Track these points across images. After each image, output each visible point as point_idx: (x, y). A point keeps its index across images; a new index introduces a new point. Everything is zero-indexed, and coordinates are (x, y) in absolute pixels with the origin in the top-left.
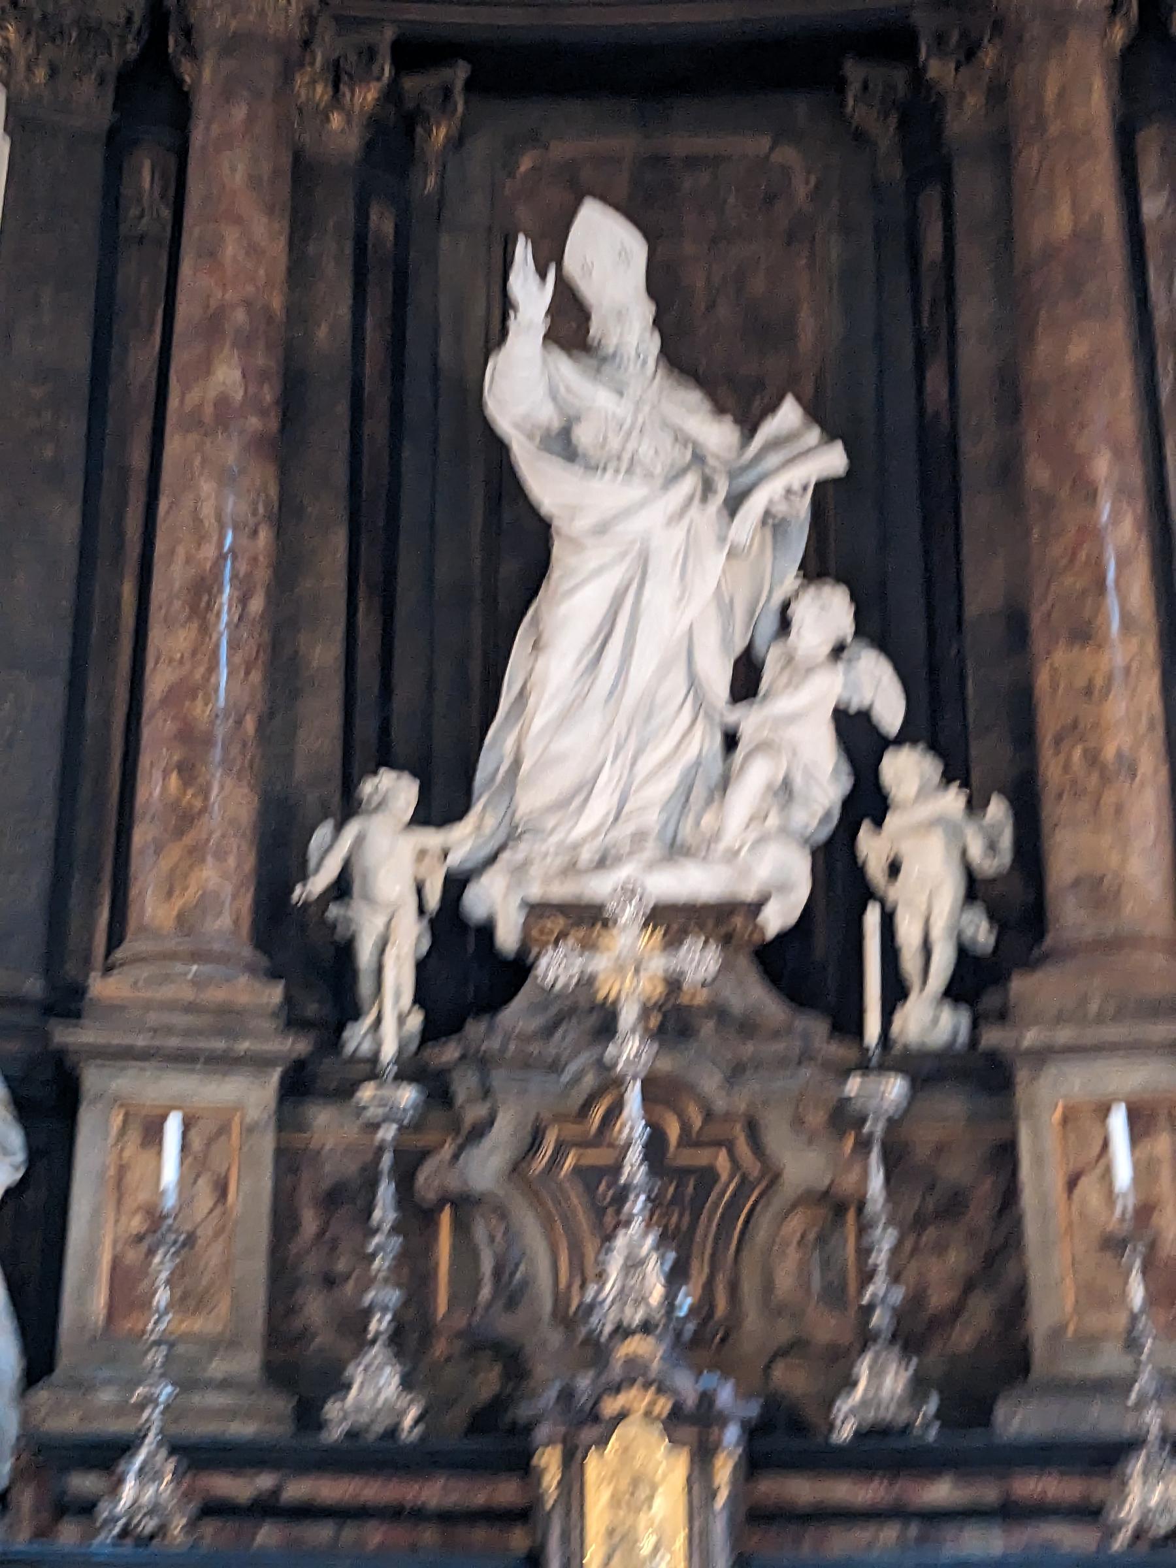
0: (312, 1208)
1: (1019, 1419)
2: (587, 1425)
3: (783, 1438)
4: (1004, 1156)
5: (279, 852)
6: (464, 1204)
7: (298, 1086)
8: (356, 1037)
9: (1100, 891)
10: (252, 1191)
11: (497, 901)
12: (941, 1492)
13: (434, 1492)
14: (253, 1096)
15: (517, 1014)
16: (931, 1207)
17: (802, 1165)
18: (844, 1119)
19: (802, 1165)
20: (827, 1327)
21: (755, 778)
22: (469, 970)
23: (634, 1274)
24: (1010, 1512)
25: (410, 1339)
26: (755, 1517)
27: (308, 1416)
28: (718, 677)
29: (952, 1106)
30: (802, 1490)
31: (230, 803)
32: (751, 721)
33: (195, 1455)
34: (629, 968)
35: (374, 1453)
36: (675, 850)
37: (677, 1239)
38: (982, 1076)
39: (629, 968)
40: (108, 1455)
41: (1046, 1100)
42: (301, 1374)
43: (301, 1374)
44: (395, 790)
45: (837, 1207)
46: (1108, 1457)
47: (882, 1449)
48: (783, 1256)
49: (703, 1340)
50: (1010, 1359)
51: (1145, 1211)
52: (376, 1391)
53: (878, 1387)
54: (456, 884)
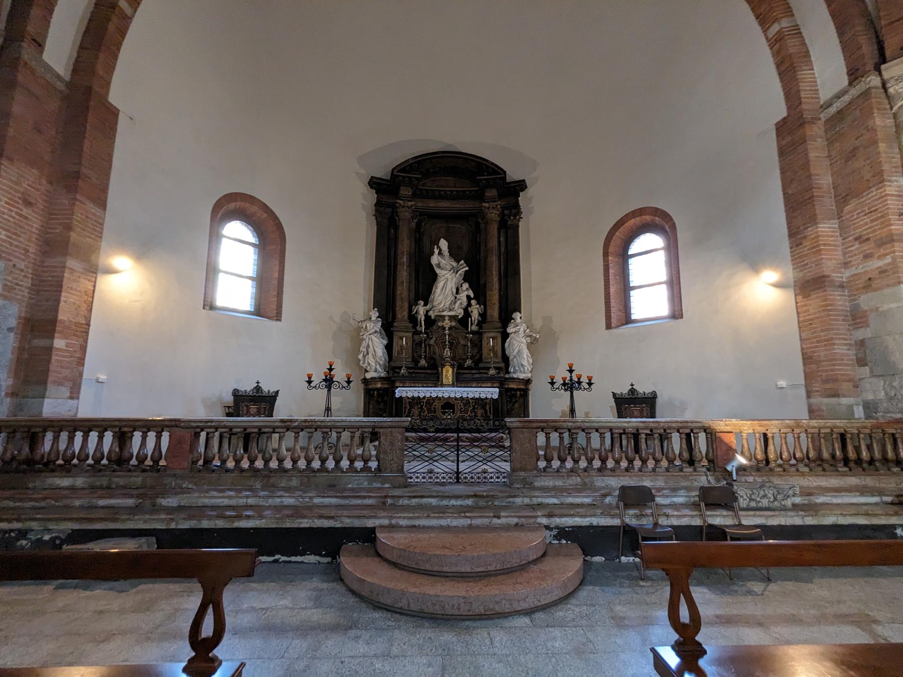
0: (417, 345)
1: (481, 365)
2: (443, 366)
3: (460, 367)
4: (481, 341)
5: (410, 310)
6: (430, 345)
7: (414, 334)
8: (418, 328)
9: (492, 316)
10: (410, 344)
11: (432, 314)
12: (474, 371)
13: (428, 371)
14: (410, 335)
15: (434, 327)
16: (474, 345)
17: (462, 342)
18: (466, 337)
19: (462, 342)
20: (464, 357)
21: (459, 302)
22: (430, 322)
23: (447, 353)
24: (480, 373)
25: (425, 358)
26: (457, 373)
27: (417, 365)
28: (454, 291)
29: (477, 336)
30: (462, 371)
31: (406, 305)
32: (458, 296)
33: (408, 368)
34: (447, 323)
35: (423, 368)
36: (450, 310)
37: (450, 349)
38: (479, 334)
39: (447, 323)
40: (400, 368)
41: (485, 336)
42: (416, 361)
43: (416, 361)
44: (422, 303)
45: (466, 345)
46: (488, 368)
47: (469, 368)
48: (460, 351)
49: (453, 358)
50: (480, 360)
51: (493, 347)
52: (423, 362)
53: (469, 362)
54: (427, 311)
